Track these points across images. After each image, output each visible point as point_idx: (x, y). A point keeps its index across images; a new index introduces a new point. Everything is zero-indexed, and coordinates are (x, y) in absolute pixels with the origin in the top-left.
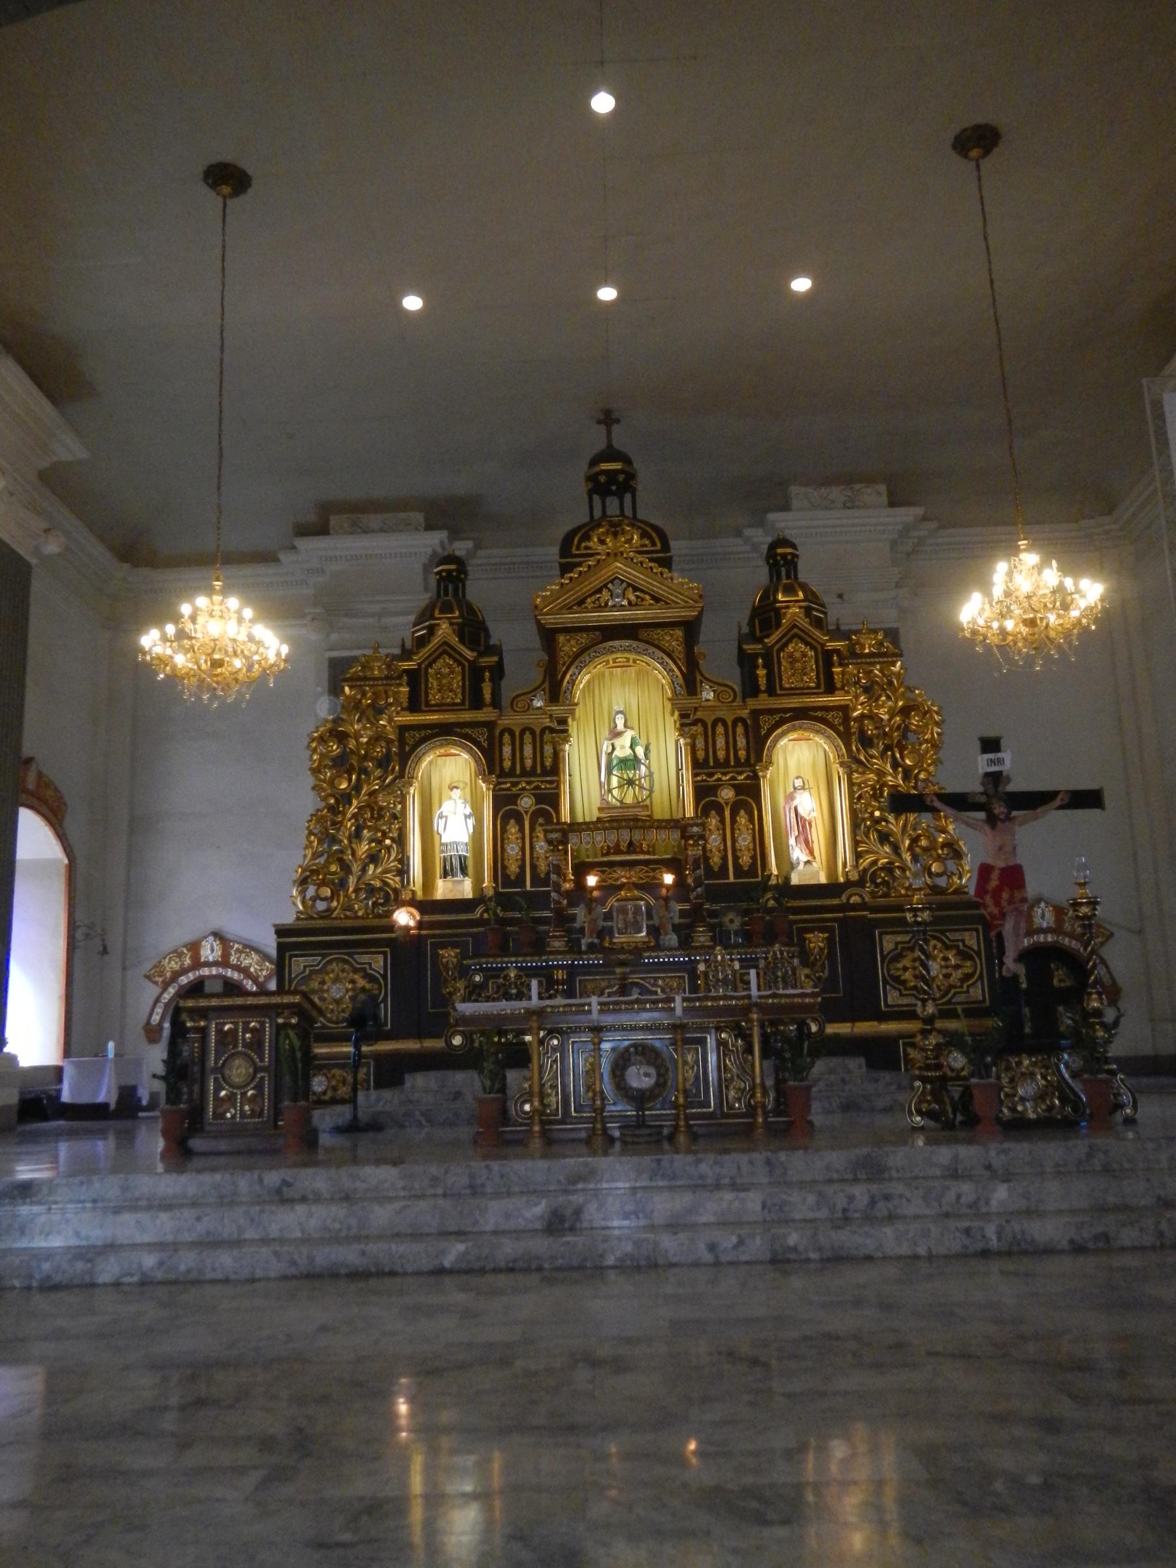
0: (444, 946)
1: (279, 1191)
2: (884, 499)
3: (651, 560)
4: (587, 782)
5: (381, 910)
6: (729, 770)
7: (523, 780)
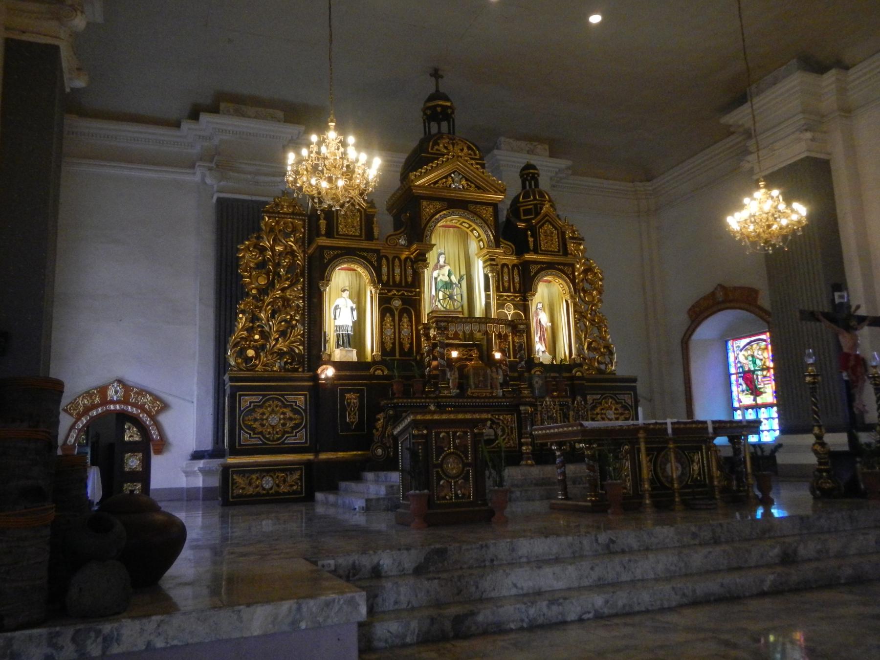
0: (349, 391)
1: (608, 546)
2: (547, 153)
3: (477, 164)
5: (289, 366)
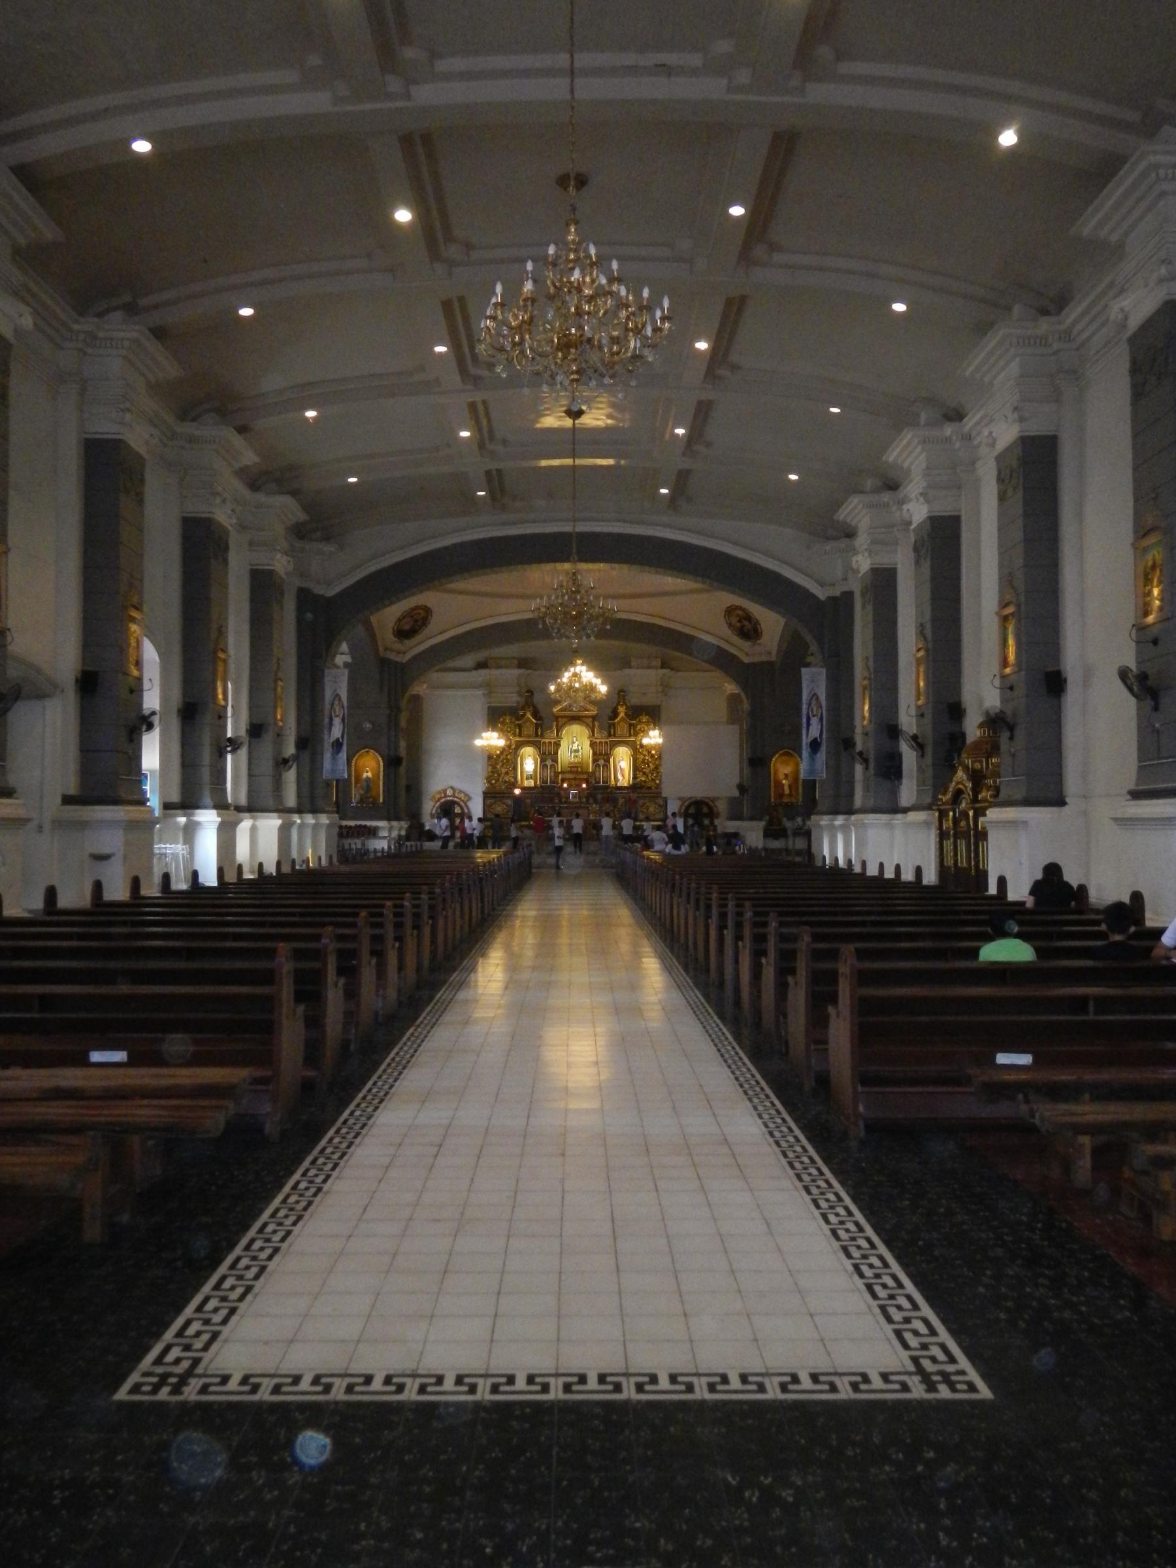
4: (565, 755)
6: (602, 756)
7: (548, 756)
